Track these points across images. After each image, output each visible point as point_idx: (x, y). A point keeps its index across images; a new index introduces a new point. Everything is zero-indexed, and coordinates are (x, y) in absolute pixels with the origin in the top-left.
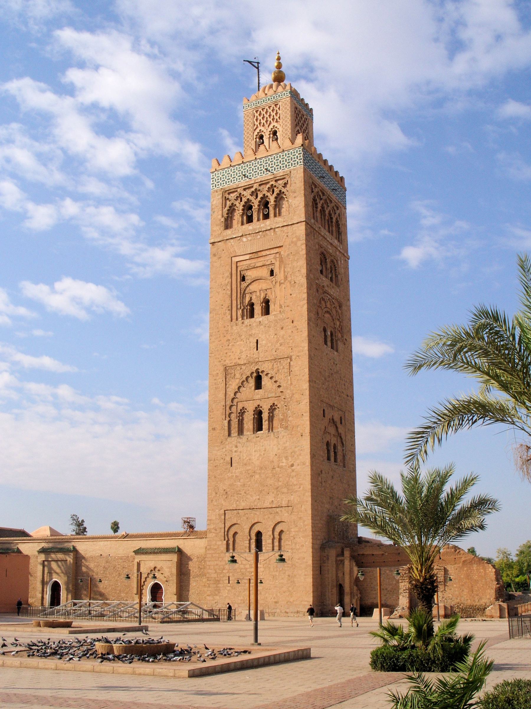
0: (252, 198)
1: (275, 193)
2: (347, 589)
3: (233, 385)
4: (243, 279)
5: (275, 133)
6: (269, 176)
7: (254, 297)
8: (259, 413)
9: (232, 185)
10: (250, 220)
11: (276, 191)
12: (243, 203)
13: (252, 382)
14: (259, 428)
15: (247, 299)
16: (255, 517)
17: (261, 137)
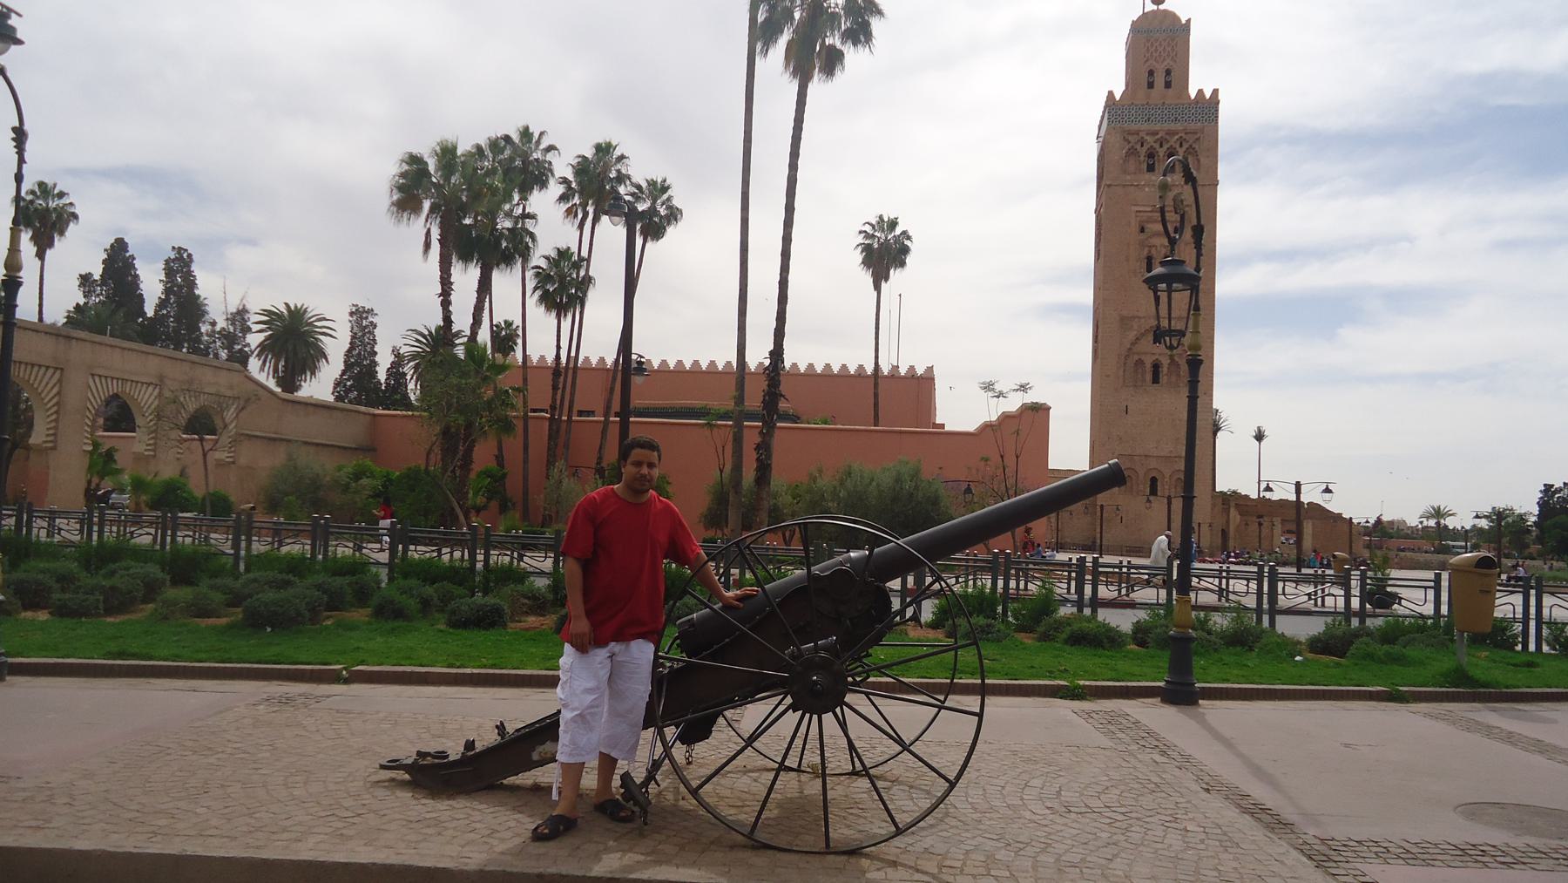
0: (1157, 146)
1: (1185, 146)
2: (1232, 533)
3: (1132, 335)
4: (1142, 230)
5: (1168, 72)
6: (1179, 126)
7: (1153, 251)
8: (1156, 367)
9: (1134, 127)
10: (1151, 168)
11: (1185, 146)
12: (1146, 147)
13: (1151, 338)
14: (1156, 380)
15: (1146, 251)
16: (1153, 464)
17: (1151, 73)
